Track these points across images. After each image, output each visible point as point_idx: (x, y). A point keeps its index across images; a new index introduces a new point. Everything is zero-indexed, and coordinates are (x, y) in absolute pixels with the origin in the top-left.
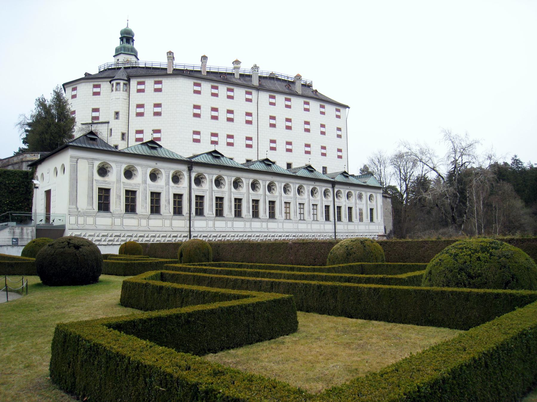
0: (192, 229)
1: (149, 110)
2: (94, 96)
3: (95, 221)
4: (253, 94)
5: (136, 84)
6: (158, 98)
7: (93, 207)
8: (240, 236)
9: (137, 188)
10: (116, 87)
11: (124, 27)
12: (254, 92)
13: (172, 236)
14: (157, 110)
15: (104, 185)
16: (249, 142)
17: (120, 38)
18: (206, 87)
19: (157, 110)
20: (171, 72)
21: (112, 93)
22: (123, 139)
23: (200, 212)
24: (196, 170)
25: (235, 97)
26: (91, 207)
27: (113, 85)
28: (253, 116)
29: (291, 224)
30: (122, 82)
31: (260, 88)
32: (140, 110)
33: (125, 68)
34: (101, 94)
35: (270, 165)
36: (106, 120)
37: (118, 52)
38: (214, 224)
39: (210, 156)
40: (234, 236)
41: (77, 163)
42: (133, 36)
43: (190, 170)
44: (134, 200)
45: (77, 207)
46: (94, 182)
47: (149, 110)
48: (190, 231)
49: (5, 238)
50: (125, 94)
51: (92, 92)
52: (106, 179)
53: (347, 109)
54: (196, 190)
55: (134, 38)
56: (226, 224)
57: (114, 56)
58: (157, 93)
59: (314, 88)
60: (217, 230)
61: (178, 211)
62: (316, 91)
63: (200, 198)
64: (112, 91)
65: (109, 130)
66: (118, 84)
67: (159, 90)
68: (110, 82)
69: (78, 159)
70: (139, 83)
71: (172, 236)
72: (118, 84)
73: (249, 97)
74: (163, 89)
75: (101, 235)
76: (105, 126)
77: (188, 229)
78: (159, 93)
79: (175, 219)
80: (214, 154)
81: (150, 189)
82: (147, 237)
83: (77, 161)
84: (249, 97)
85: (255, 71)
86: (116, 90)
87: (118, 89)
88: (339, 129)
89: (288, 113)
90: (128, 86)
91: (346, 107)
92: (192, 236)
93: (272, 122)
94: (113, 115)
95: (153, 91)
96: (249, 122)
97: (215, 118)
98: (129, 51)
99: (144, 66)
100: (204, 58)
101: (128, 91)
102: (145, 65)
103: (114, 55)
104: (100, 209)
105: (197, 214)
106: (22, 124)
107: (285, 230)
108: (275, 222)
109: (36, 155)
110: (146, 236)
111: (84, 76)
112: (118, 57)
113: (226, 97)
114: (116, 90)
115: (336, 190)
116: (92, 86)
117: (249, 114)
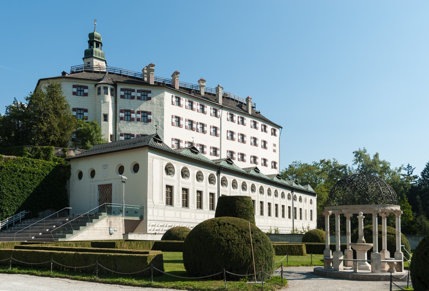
3: (164, 213)
7: (163, 201)
9: (189, 186)
21: (99, 96)
26: (162, 201)
27: (99, 89)
33: (109, 73)
43: (218, 174)
45: (153, 201)
57: (83, 59)
68: (96, 85)
72: (106, 88)
88: (275, 145)
103: (83, 57)
111: (61, 75)
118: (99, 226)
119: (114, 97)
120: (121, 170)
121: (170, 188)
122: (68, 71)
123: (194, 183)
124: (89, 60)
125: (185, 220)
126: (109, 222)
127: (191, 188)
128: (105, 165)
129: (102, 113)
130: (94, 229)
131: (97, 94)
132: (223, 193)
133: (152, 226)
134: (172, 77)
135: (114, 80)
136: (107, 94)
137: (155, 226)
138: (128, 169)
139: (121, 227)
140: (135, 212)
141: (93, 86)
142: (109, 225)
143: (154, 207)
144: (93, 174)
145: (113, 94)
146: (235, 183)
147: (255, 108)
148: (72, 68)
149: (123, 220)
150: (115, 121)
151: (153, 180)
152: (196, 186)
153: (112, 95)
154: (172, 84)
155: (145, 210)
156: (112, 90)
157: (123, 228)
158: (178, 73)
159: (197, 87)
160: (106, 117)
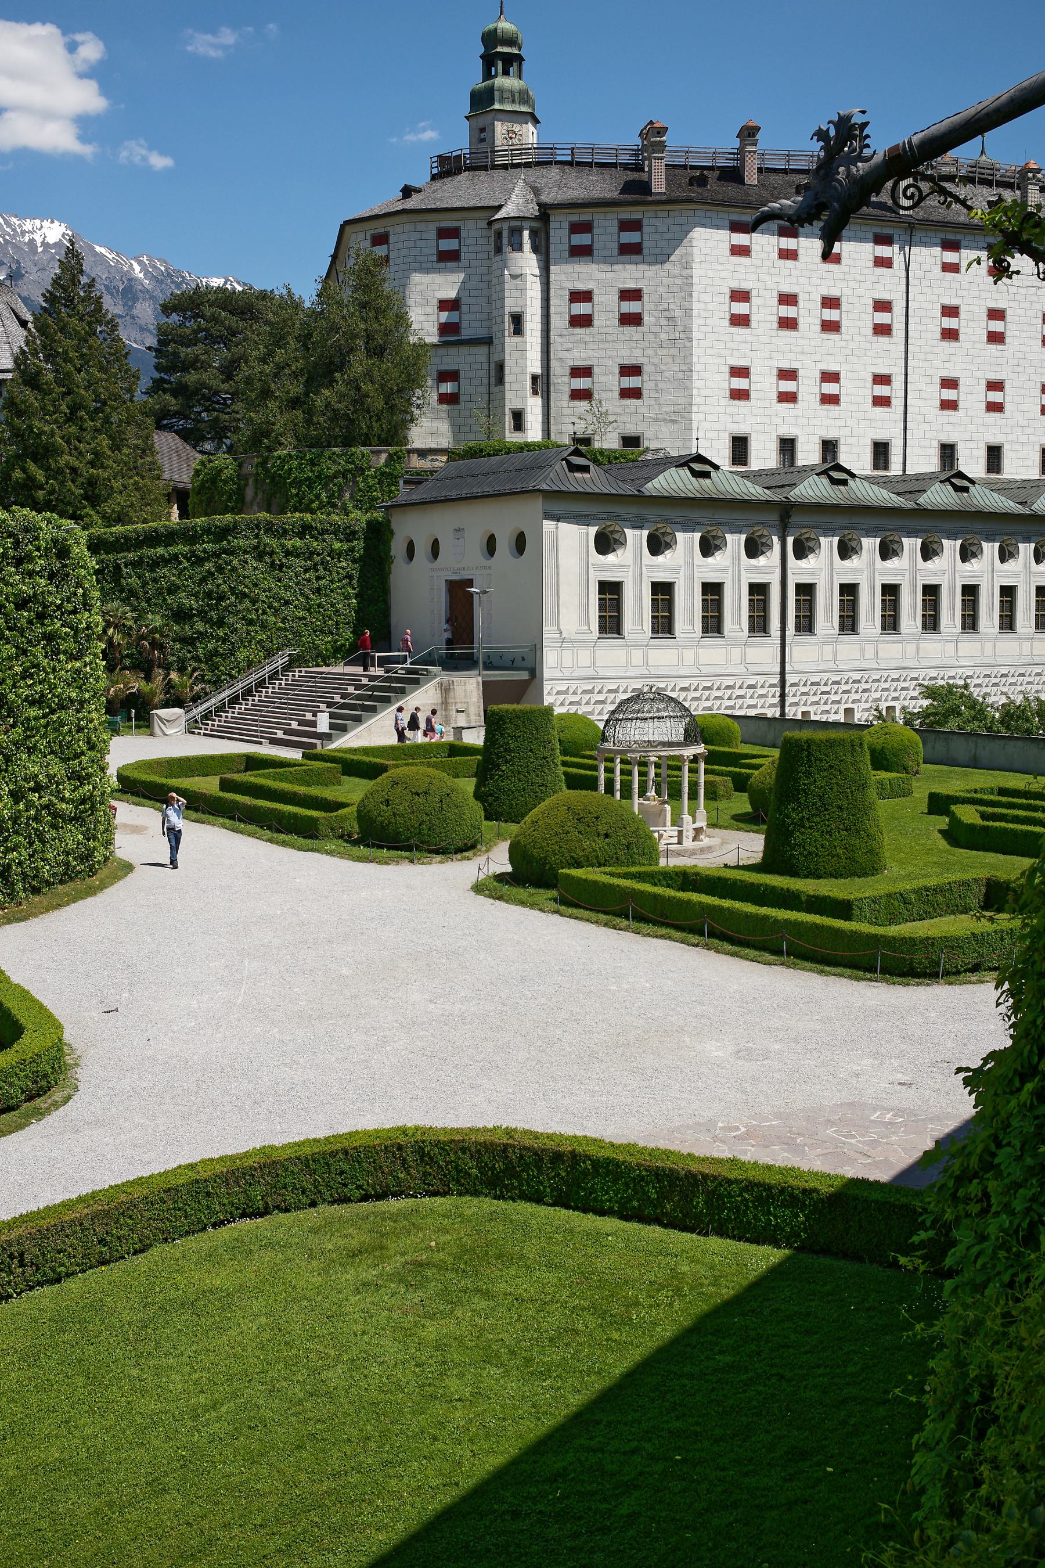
0: (788, 668)
3: (594, 658)
8: (893, 680)
13: (745, 686)
15: (608, 574)
20: (663, 190)
22: (535, 392)
23: (806, 624)
27: (499, 235)
28: (895, 309)
29: (1015, 645)
35: (966, 490)
36: (483, 333)
38: (835, 653)
39: (825, 481)
40: (878, 681)
42: (520, 48)
44: (670, 605)
45: (559, 630)
48: (783, 673)
52: (611, 558)
54: (800, 570)
55: (522, 53)
56: (863, 650)
57: (467, 118)
60: (842, 666)
61: (759, 625)
63: (806, 591)
65: (493, 366)
68: (490, 224)
71: (745, 686)
75: (605, 690)
76: (478, 354)
77: (778, 669)
79: (751, 646)
80: (835, 475)
81: (700, 575)
82: (696, 690)
90: (543, 236)
92: (788, 684)
93: (950, 323)
97: (788, 324)
98: (514, 101)
99: (569, 158)
100: (749, 133)
104: (603, 629)
105: (798, 628)
107: (1000, 661)
108: (975, 640)
110: (693, 688)
116: (434, 235)
117: (882, 306)
122: (420, 178)
123: (691, 565)
124: (482, 121)
125: (662, 672)
129: (507, 310)
133: (559, 693)
135: (544, 198)
136: (519, 248)
137: (566, 692)
141: (483, 224)
143: (563, 644)
144: (435, 549)
153: (535, 249)
155: (538, 654)
156: (534, 234)
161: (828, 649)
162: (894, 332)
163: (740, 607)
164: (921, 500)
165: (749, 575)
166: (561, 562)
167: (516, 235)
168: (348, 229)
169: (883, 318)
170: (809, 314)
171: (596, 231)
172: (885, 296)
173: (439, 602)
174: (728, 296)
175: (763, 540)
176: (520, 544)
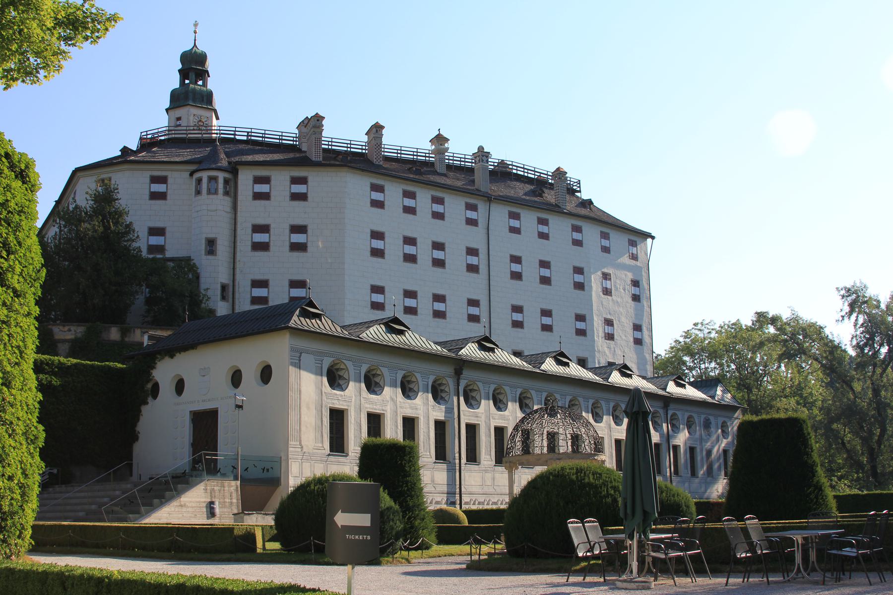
0: (463, 489)
1: (280, 238)
2: (153, 202)
4: (479, 210)
5: (251, 182)
6: (298, 213)
10: (208, 186)
11: (188, 47)
12: (482, 206)
14: (298, 238)
16: (474, 311)
17: (179, 71)
18: (393, 192)
19: (298, 238)
21: (199, 197)
22: (224, 298)
23: (473, 457)
24: (468, 375)
25: (446, 215)
26: (321, 445)
27: (199, 181)
30: (221, 176)
31: (489, 199)
32: (260, 238)
34: (168, 197)
37: (178, 99)
38: (494, 479)
41: (300, 360)
43: (458, 373)
45: (300, 444)
46: (324, 398)
47: (280, 238)
49: (199, 502)
50: (228, 201)
51: (148, 193)
53: (649, 240)
57: (167, 110)
58: (296, 203)
59: (584, 195)
62: (590, 202)
63: (472, 429)
64: (198, 192)
66: (212, 179)
67: (302, 197)
68: (191, 174)
69: (301, 353)
70: (258, 180)
73: (471, 215)
74: (309, 195)
78: (302, 203)
83: (300, 357)
84: (471, 215)
85: (483, 161)
86: (209, 192)
87: (213, 191)
89: (544, 250)
91: (646, 235)
94: (203, 246)
95: (288, 198)
96: (472, 269)
99: (245, 138)
101: (232, 194)
102: (247, 136)
103: (167, 105)
106: (371, 309)
109: (73, 328)
112: (179, 112)
113: (401, 210)
114: (209, 192)
115: (670, 413)
116: (148, 180)
118: (190, 500)
119: (231, 197)
120: (236, 378)
121: (337, 418)
126: (209, 491)
127: (389, 411)
128: (205, 369)
130: (181, 506)
131: (194, 194)
132: (469, 420)
134: (367, 136)
138: (250, 376)
139: (235, 501)
140: (264, 470)
142: (209, 497)
144: (180, 387)
145: (228, 191)
146: (502, 393)
147: (580, 191)
148: (143, 134)
149: (237, 486)
150: (236, 249)
151: (300, 399)
152: (401, 407)
153: (226, 193)
154: (367, 152)
156: (226, 182)
157: (238, 503)
158: (380, 127)
159: (429, 154)
160: (213, 244)
161: (489, 476)
162: (480, 271)
163: (429, 439)
164: (542, 368)
165: (434, 413)
166: (302, 389)
167: (213, 182)
168: (79, 174)
169: (473, 260)
170: (424, 252)
171: (273, 182)
172: (473, 245)
173: (184, 432)
174: (369, 235)
175: (442, 388)
176: (266, 374)
